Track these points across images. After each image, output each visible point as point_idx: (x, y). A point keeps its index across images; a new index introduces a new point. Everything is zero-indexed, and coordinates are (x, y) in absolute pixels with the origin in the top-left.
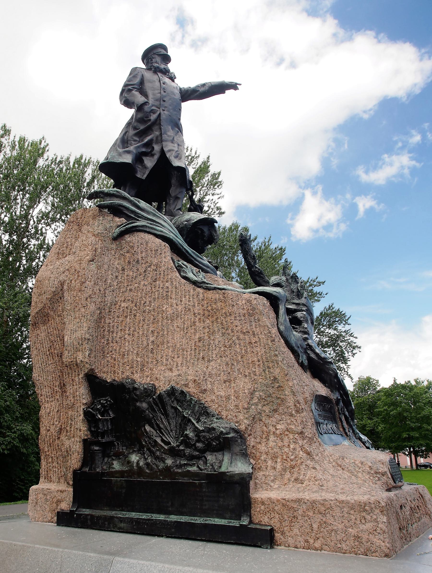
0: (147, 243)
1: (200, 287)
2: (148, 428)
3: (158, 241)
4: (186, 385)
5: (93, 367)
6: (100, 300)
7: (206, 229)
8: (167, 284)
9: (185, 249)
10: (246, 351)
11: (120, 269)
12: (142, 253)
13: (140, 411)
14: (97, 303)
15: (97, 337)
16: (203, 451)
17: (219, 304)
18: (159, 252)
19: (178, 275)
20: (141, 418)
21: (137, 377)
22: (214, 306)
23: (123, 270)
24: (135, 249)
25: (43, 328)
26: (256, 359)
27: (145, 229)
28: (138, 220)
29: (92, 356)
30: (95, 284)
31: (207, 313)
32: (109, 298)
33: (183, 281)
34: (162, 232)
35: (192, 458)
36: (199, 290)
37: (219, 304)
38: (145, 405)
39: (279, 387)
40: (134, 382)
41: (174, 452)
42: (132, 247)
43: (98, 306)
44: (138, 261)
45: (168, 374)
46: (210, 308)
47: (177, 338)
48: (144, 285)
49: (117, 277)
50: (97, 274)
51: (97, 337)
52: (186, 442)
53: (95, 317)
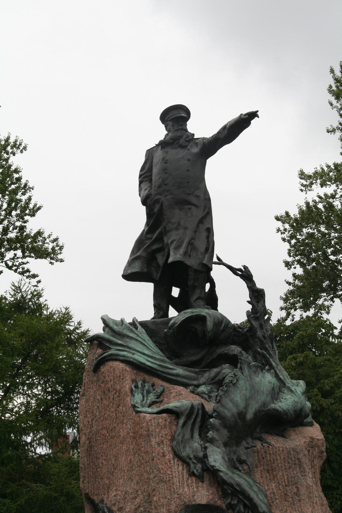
0: (114, 370)
3: (122, 365)
5: (87, 492)
6: (88, 431)
7: (199, 328)
9: (148, 366)
11: (100, 399)
12: (111, 381)
14: (87, 434)
15: (89, 464)
18: (121, 377)
23: (102, 400)
24: (107, 378)
27: (112, 358)
28: (111, 348)
29: (85, 482)
30: (84, 417)
34: (124, 356)
42: (105, 377)
43: (88, 437)
44: (109, 389)
47: (123, 461)
48: (112, 412)
49: (98, 407)
50: (85, 407)
51: (89, 464)
53: (86, 447)
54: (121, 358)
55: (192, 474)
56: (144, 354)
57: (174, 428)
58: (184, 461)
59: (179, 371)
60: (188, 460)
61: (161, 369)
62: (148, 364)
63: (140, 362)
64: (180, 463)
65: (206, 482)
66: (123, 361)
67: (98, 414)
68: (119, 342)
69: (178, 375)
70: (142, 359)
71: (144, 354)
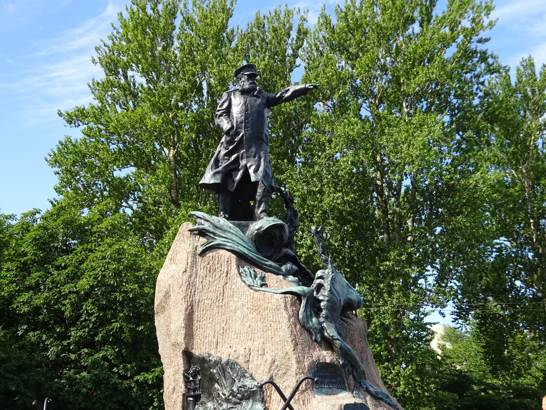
1: (252, 289)
2: (216, 386)
3: (229, 253)
4: (238, 358)
8: (233, 287)
10: (274, 335)
13: (212, 374)
16: (241, 399)
17: (261, 301)
19: (240, 279)
20: (212, 380)
21: (212, 352)
22: (259, 303)
25: (162, 316)
26: (279, 340)
31: (254, 308)
32: (197, 298)
33: (243, 284)
35: (236, 404)
36: (251, 291)
37: (261, 301)
38: (215, 371)
39: (289, 358)
40: (210, 355)
41: (227, 401)
45: (230, 350)
46: (256, 305)
47: (237, 326)
52: (232, 394)
54: (228, 248)
55: (316, 341)
56: (245, 247)
57: (298, 305)
58: (308, 331)
59: (270, 263)
60: (311, 330)
61: (259, 260)
62: (250, 255)
63: (244, 253)
64: (306, 332)
65: (323, 347)
66: (229, 250)
67: (201, 287)
68: (224, 235)
69: (270, 266)
70: (246, 251)
71: (245, 247)
